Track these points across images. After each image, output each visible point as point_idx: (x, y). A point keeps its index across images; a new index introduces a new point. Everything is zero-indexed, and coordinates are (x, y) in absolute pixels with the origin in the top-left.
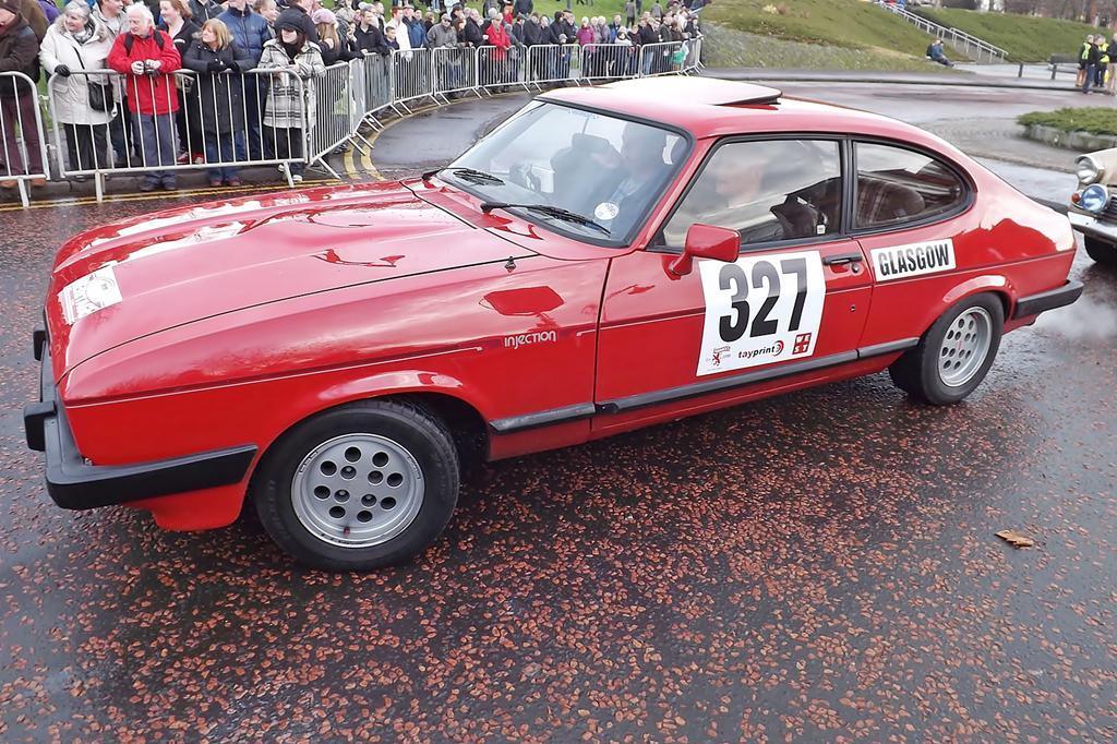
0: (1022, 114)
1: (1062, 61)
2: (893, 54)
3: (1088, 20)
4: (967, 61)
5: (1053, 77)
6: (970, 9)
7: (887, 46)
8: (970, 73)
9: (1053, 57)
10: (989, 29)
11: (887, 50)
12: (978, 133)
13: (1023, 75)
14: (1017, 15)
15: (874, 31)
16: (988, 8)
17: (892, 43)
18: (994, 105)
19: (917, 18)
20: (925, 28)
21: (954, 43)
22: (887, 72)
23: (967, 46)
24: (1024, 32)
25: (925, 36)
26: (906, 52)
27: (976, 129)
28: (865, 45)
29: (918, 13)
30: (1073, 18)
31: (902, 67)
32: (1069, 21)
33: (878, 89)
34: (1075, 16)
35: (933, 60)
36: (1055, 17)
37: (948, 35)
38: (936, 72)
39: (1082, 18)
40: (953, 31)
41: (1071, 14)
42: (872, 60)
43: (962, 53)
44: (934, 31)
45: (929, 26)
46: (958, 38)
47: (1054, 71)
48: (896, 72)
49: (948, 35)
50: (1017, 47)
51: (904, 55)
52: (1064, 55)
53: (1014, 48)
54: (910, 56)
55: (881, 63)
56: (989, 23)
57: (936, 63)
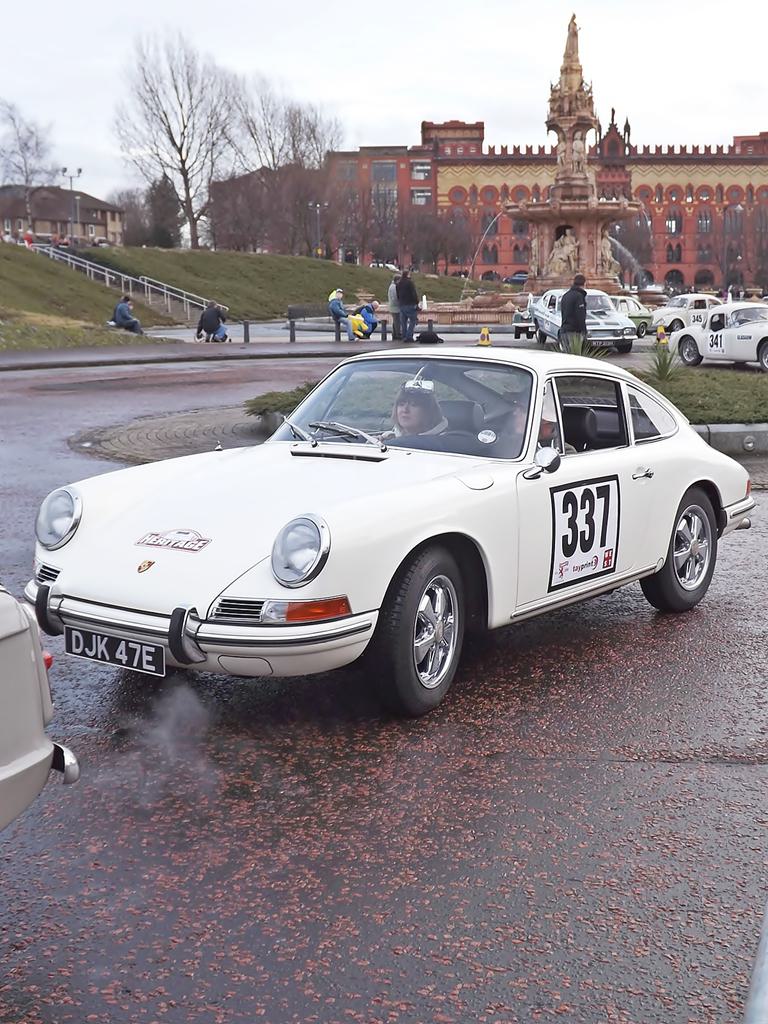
0: (253, 398)
1: (304, 314)
2: (55, 321)
3: (330, 255)
4: (171, 323)
5: (293, 339)
6: (165, 247)
7: (47, 311)
8: (175, 342)
9: (290, 310)
10: (196, 275)
11: (45, 317)
12: (194, 434)
13: (252, 340)
14: (233, 251)
15: (24, 288)
16: (190, 244)
17: (54, 305)
18: (216, 387)
19: (87, 265)
20: (103, 278)
21: (149, 299)
22: (50, 351)
23: (168, 301)
24: (246, 277)
25: (104, 291)
26: (78, 318)
27: (192, 427)
28: (12, 311)
29: (88, 256)
30: (309, 253)
31: (71, 342)
32: (304, 257)
33: (37, 378)
34: (311, 251)
35: (119, 326)
36: (283, 253)
37: (138, 287)
38: (124, 344)
39: (320, 252)
40: (144, 280)
41: (305, 245)
42: (23, 333)
43: (162, 314)
44: (116, 282)
45: (107, 276)
46: (153, 291)
47: (292, 329)
48: (64, 349)
49: (138, 287)
50: (238, 298)
51: (71, 322)
52: (306, 306)
53: (236, 301)
54: (82, 323)
55: (39, 337)
56: (195, 264)
57: (122, 331)
